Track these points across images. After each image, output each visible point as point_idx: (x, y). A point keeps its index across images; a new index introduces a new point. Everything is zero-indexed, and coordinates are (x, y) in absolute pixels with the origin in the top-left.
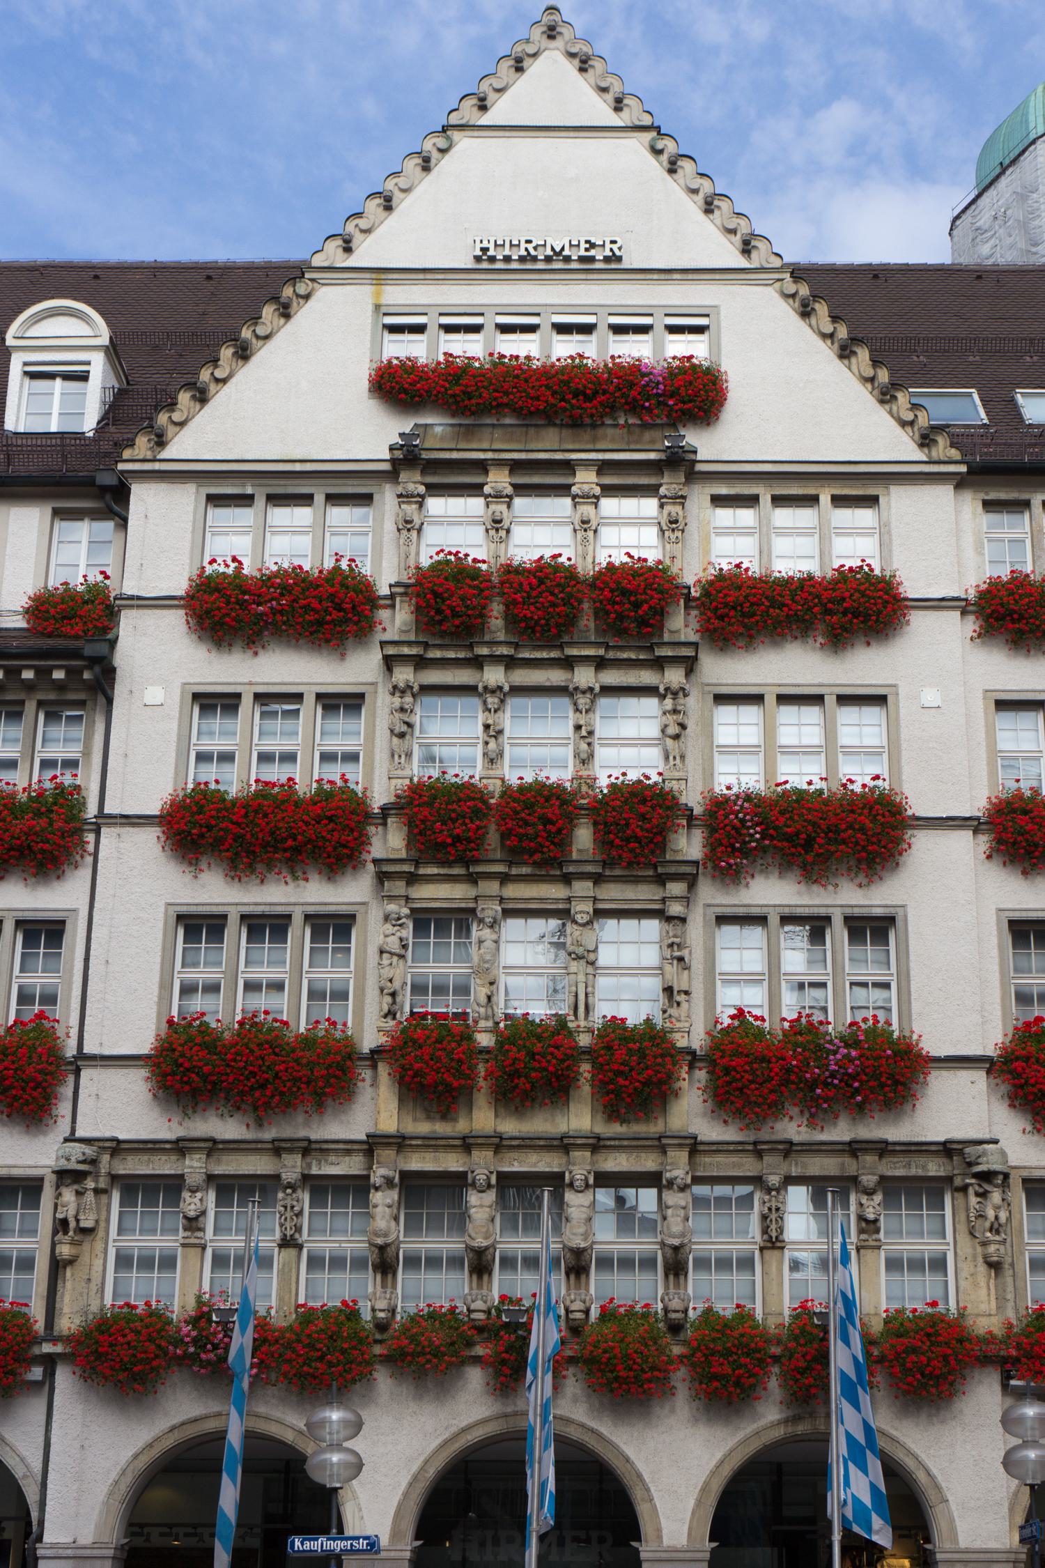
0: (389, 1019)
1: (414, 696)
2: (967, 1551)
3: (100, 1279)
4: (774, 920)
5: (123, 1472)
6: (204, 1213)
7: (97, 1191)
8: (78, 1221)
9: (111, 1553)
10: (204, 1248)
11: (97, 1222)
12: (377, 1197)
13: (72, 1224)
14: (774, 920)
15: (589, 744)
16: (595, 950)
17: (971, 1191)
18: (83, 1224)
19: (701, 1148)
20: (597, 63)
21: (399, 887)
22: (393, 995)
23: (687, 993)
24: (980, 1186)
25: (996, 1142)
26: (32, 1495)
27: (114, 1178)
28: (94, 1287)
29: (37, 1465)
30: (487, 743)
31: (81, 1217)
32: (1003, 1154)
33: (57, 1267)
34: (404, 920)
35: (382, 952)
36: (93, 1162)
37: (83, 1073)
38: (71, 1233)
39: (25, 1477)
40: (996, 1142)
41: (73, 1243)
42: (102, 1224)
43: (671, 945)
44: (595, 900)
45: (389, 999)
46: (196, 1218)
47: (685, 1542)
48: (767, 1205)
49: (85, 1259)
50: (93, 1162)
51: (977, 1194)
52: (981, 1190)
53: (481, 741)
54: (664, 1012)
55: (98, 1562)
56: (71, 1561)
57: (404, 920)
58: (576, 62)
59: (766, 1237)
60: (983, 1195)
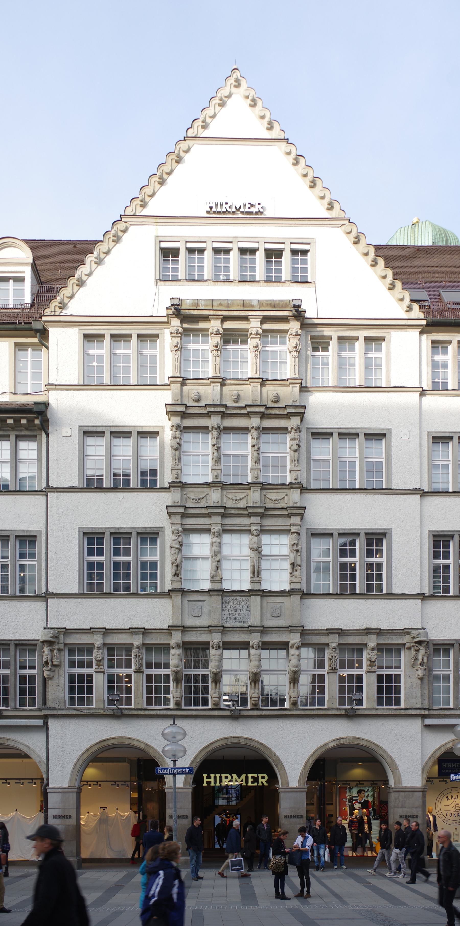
0: (176, 577)
1: (181, 431)
2: (406, 788)
3: (63, 686)
4: (335, 535)
5: (78, 760)
6: (103, 659)
7: (60, 650)
8: (52, 662)
9: (76, 790)
10: (104, 673)
11: (60, 662)
12: (172, 651)
13: (50, 663)
14: (335, 535)
15: (258, 454)
16: (261, 547)
17: (413, 649)
18: (55, 663)
19: (305, 632)
20: (259, 103)
21: (177, 519)
22: (177, 566)
23: (300, 566)
24: (417, 647)
25: (424, 629)
26: (43, 769)
27: (65, 644)
28: (61, 688)
29: (45, 758)
30: (214, 453)
31: (54, 661)
32: (427, 633)
33: (45, 681)
34: (180, 534)
35: (171, 548)
36: (57, 637)
37: (49, 600)
38: (50, 667)
39: (40, 762)
40: (424, 629)
41: (51, 670)
42: (63, 663)
43: (293, 545)
44: (261, 525)
45: (175, 568)
46: (100, 661)
47: (297, 785)
48: (331, 655)
49: (56, 677)
50: (57, 637)
51: (415, 650)
52: (417, 648)
53: (211, 453)
54: (291, 574)
55: (71, 794)
56: (60, 794)
57: (180, 534)
58: (249, 102)
59: (330, 668)
60: (418, 651)
